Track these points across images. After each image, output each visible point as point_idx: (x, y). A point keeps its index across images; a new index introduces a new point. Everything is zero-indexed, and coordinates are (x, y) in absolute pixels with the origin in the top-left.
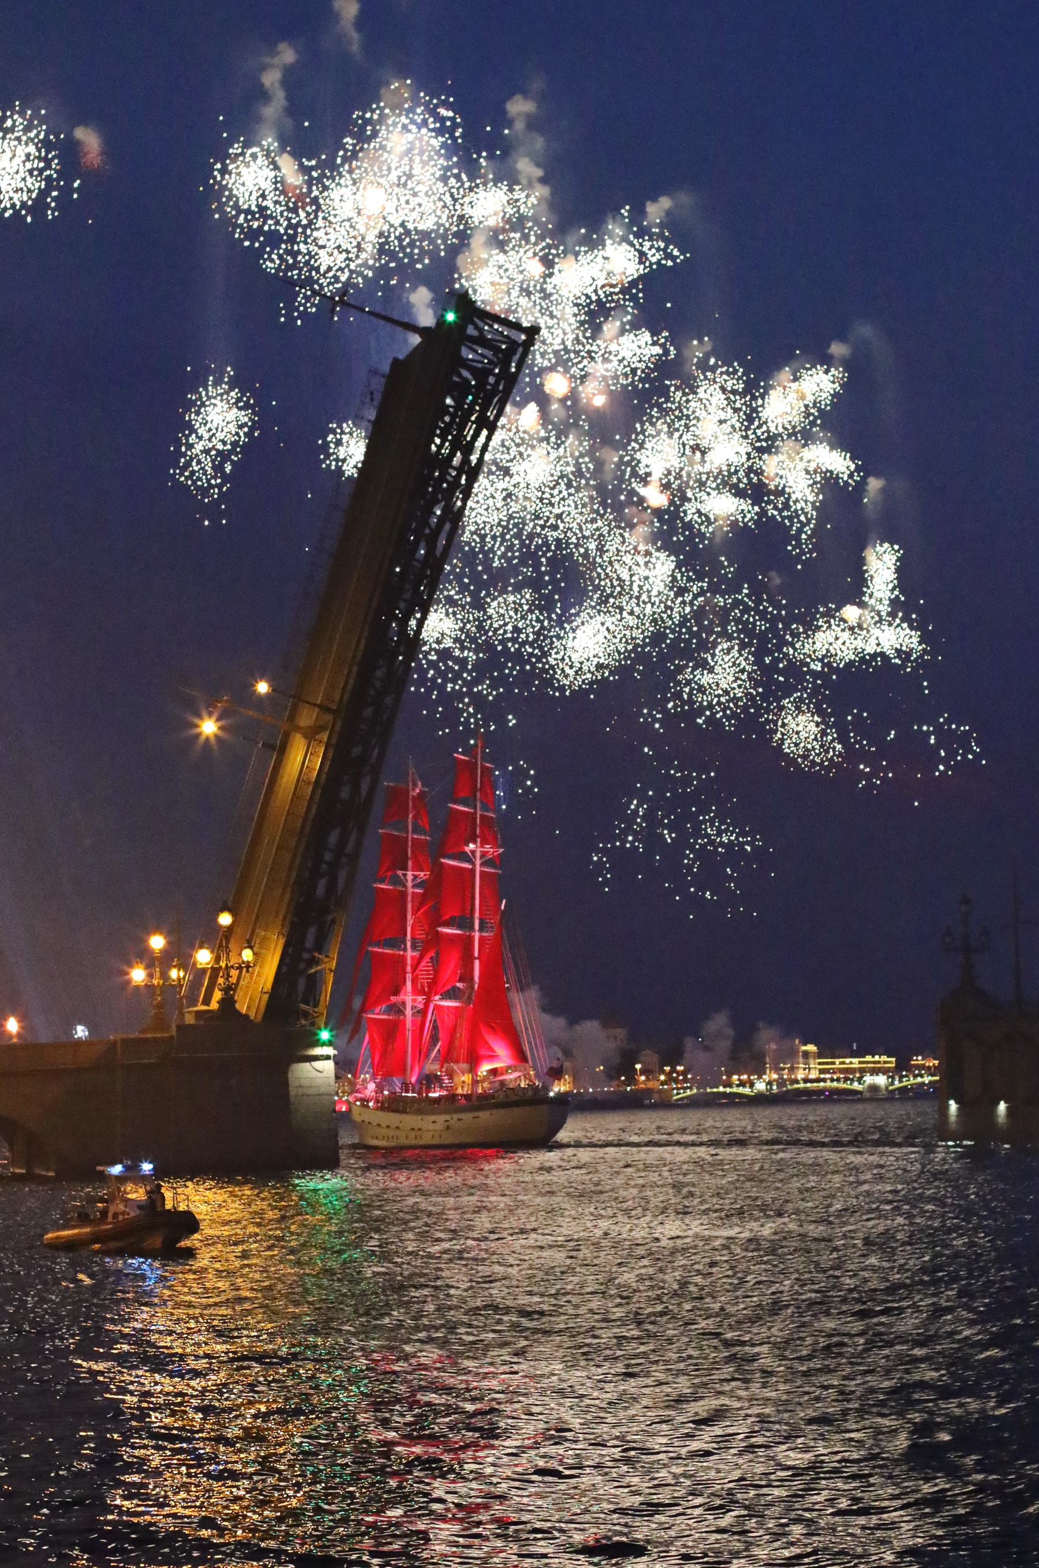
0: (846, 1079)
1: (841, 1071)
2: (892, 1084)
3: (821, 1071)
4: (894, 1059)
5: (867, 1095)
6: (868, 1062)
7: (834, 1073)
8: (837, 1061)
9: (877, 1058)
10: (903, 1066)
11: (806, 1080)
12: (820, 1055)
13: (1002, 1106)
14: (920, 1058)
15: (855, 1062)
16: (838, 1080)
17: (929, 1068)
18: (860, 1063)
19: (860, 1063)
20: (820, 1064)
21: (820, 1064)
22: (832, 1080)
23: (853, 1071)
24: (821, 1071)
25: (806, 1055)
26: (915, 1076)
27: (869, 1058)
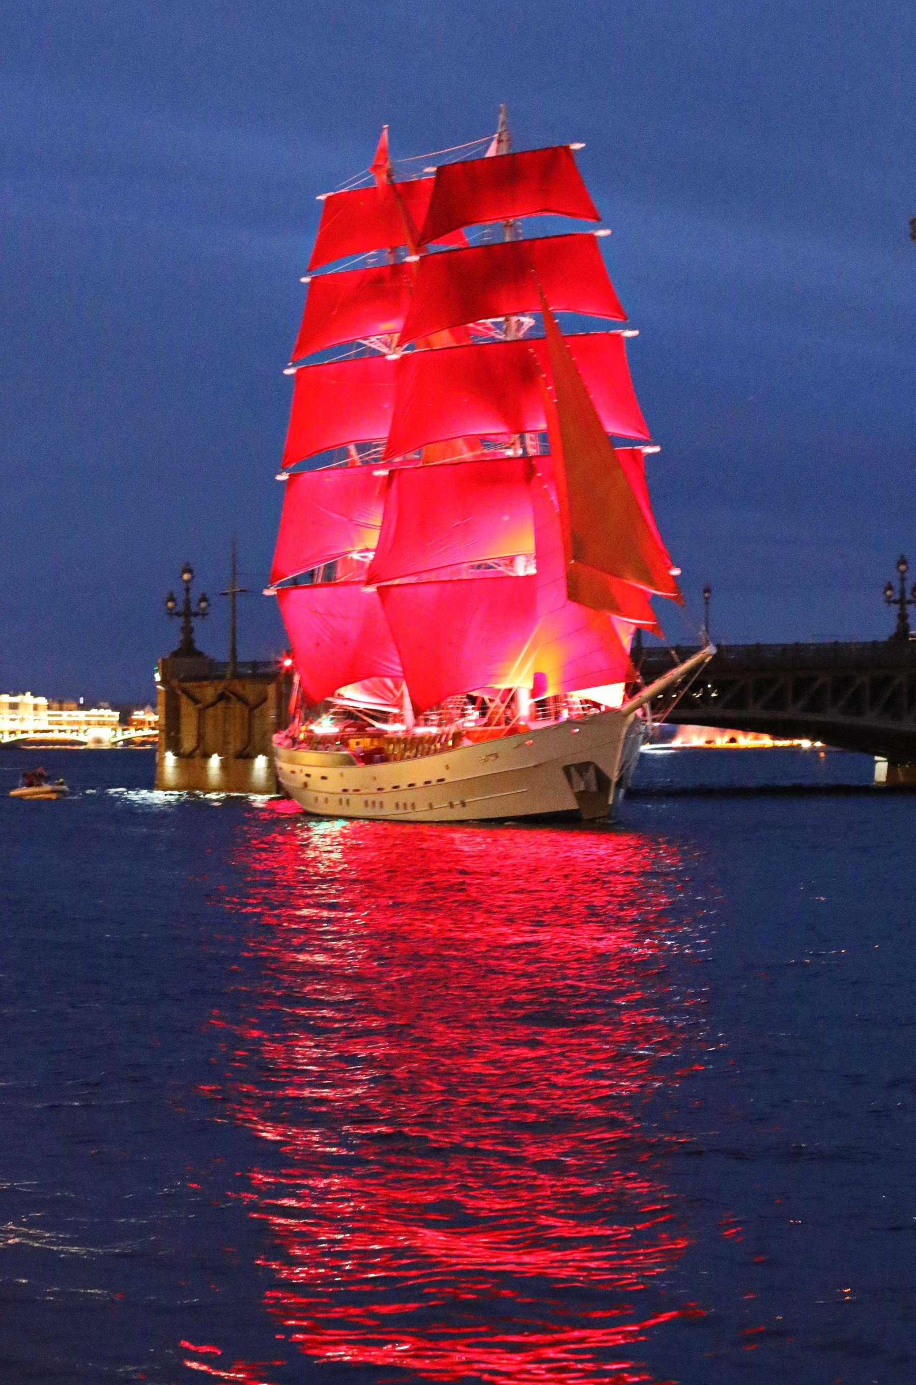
0: (72, 731)
1: (70, 723)
2: (115, 736)
3: (50, 723)
4: (117, 714)
5: (91, 746)
6: (94, 716)
7: (61, 724)
8: (65, 714)
9: (102, 711)
10: (125, 721)
11: (35, 732)
12: (49, 708)
13: (215, 762)
14: (142, 713)
15: (81, 715)
16: (65, 731)
17: (150, 723)
18: (87, 716)
19: (87, 716)
20: (49, 715)
21: (49, 715)
22: (60, 731)
23: (79, 723)
24: (50, 723)
25: (36, 707)
26: (137, 730)
27: (94, 711)
